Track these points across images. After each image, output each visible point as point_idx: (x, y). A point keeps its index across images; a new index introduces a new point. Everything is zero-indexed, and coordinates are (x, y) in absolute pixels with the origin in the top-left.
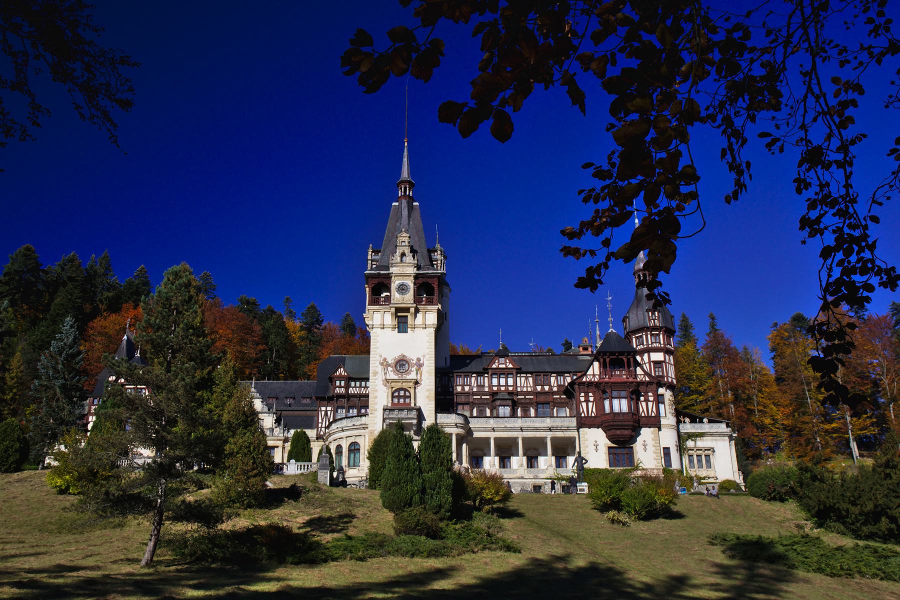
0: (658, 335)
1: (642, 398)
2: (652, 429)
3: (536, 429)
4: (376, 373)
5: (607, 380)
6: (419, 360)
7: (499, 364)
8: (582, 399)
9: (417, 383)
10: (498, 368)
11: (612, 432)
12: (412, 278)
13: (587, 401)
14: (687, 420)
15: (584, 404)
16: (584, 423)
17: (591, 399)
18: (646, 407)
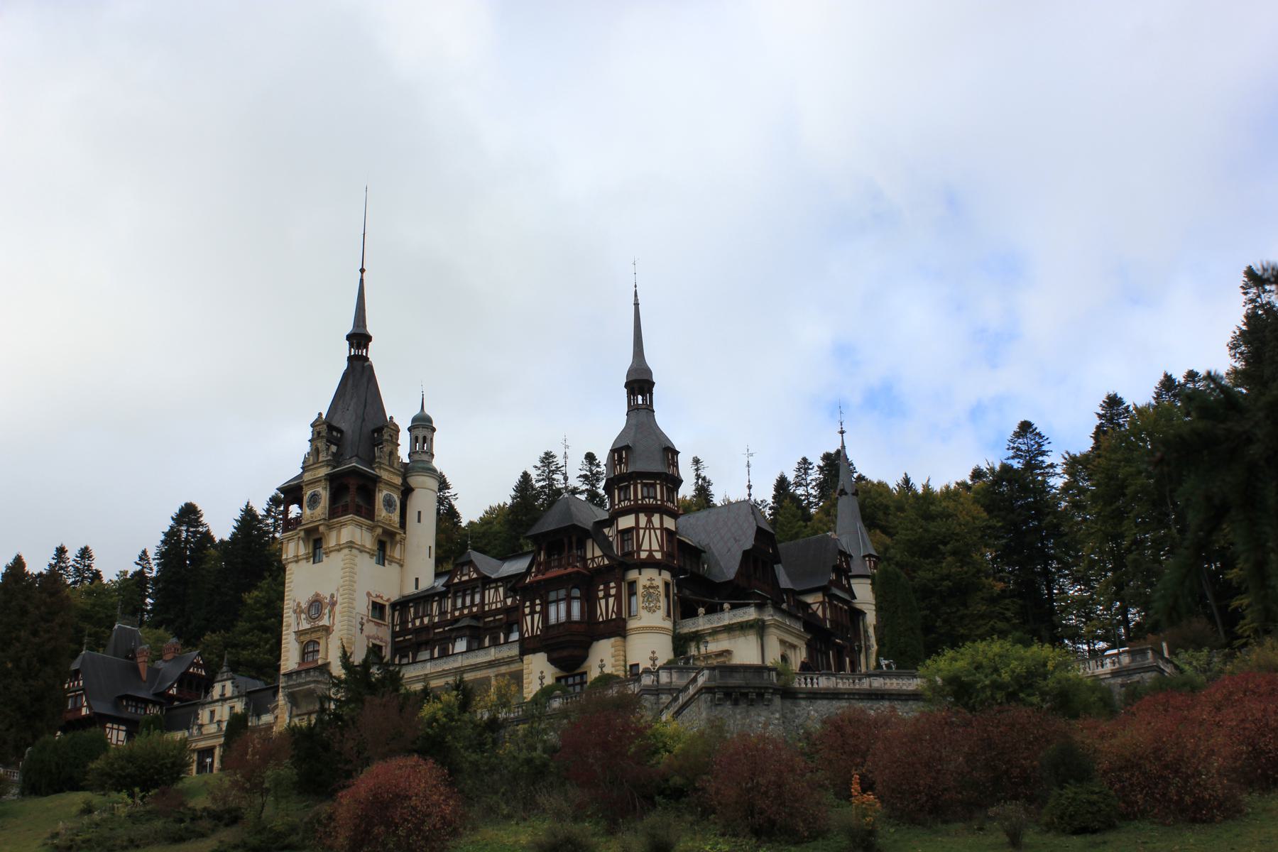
0: (628, 487)
1: (601, 594)
2: (613, 640)
3: (475, 668)
4: (289, 626)
5: (540, 577)
6: (332, 596)
7: (463, 575)
8: (527, 611)
9: (327, 630)
10: (461, 583)
11: (555, 655)
12: (323, 483)
13: (533, 613)
14: (701, 610)
15: (529, 618)
16: (527, 647)
17: (538, 608)
18: (605, 608)
